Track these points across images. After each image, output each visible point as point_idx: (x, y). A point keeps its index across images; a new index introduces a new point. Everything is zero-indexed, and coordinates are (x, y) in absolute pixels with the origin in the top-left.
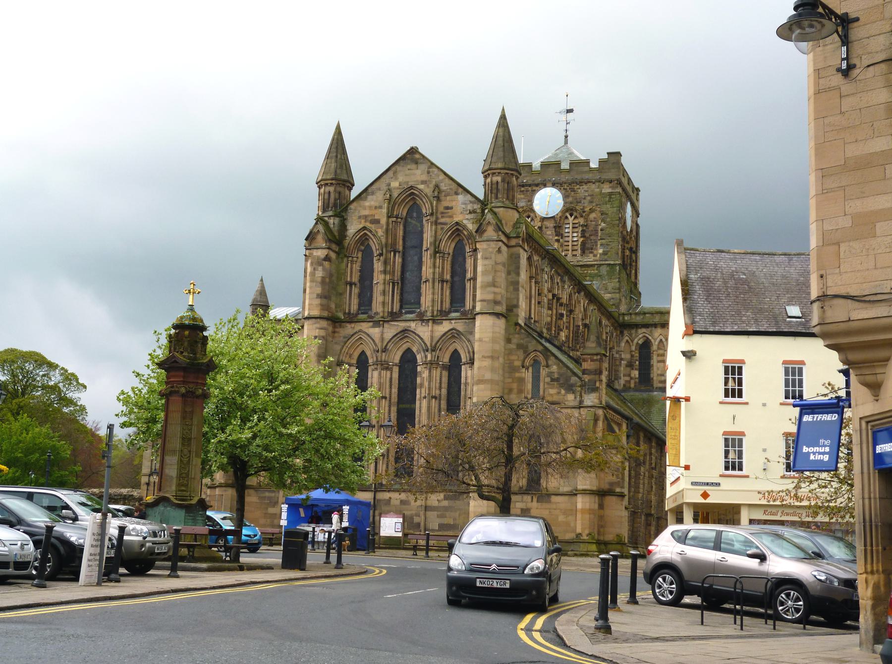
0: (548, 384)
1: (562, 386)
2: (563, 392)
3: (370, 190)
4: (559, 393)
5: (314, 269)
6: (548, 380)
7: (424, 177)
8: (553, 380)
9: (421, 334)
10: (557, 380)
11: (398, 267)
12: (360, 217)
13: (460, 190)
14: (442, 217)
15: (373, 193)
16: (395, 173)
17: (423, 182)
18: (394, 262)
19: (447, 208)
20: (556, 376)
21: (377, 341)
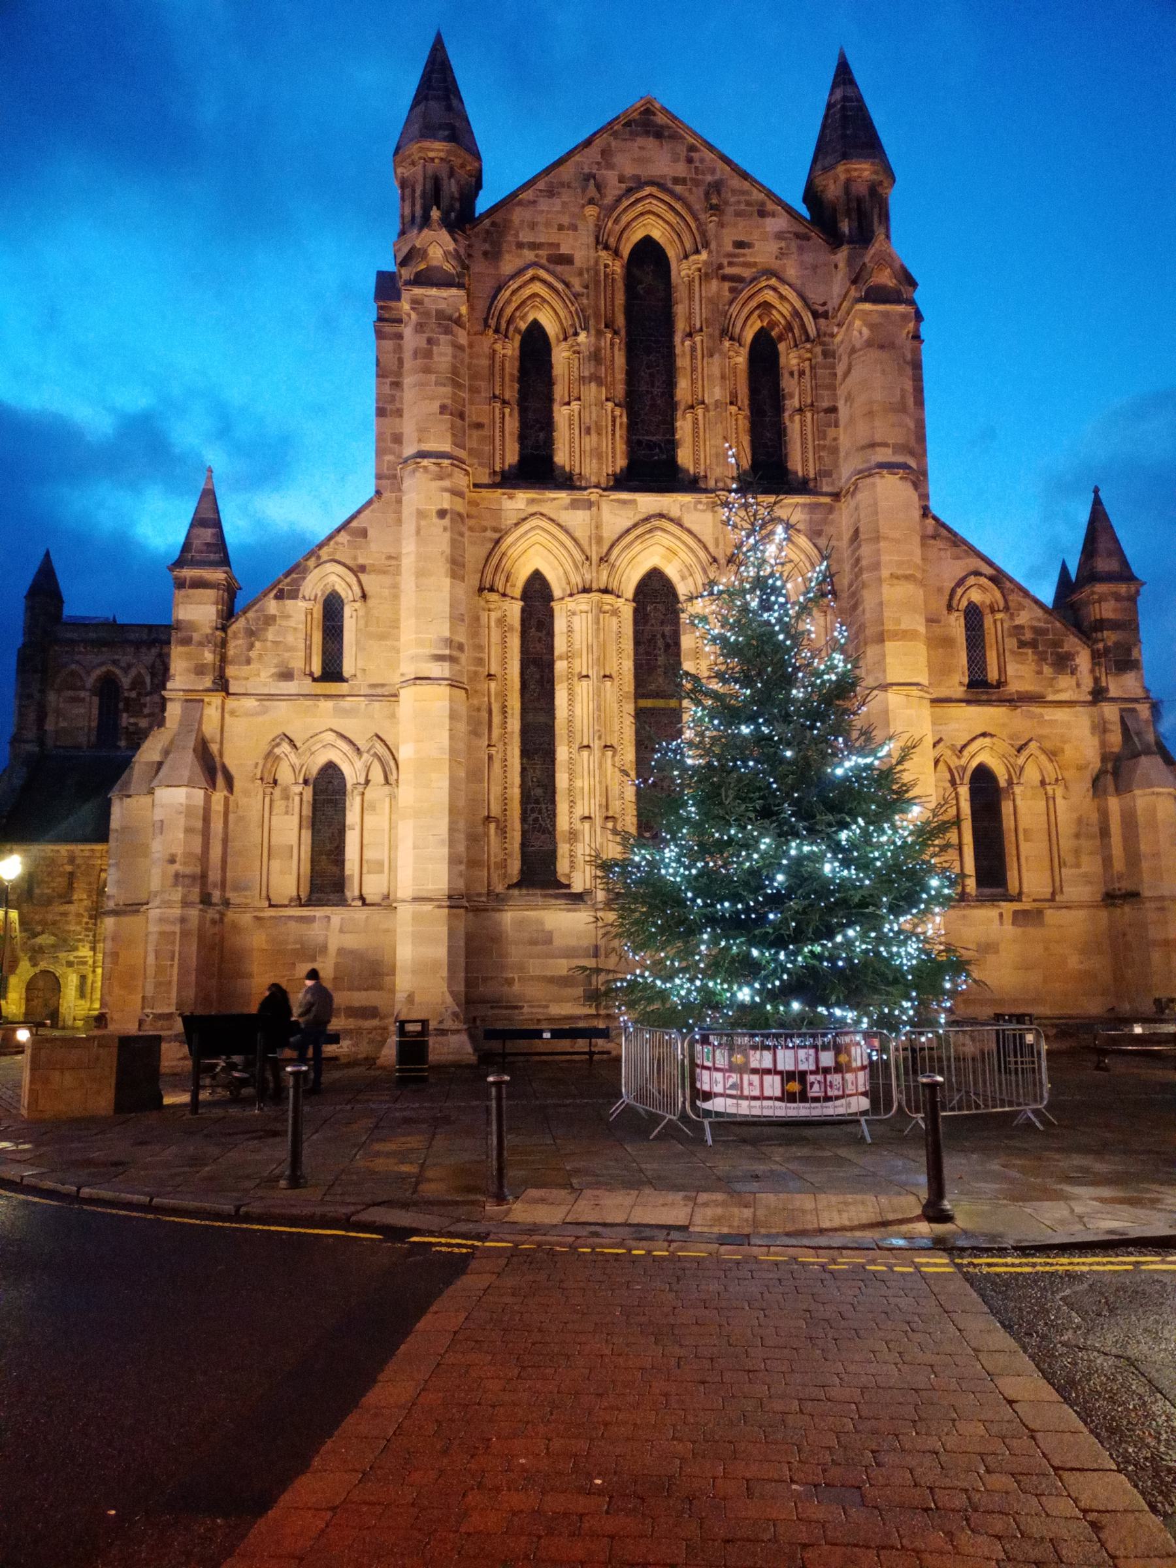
0: (1012, 652)
1: (1041, 658)
2: (1047, 670)
3: (541, 185)
4: (1040, 672)
5: (430, 341)
6: (1011, 643)
7: (681, 169)
8: (1022, 644)
9: (695, 528)
10: (1033, 644)
11: (620, 376)
12: (520, 245)
13: (771, 206)
14: (730, 264)
15: (551, 193)
16: (605, 153)
17: (676, 181)
18: (613, 361)
19: (740, 245)
20: (1028, 636)
21: (585, 543)
